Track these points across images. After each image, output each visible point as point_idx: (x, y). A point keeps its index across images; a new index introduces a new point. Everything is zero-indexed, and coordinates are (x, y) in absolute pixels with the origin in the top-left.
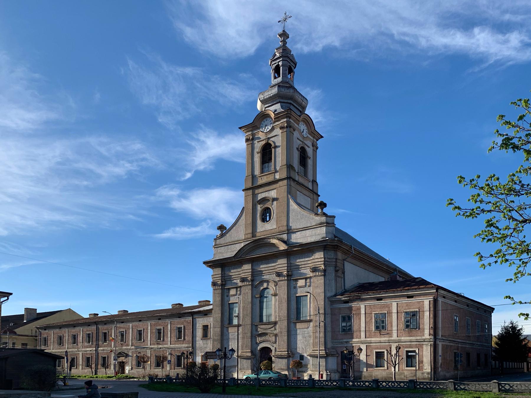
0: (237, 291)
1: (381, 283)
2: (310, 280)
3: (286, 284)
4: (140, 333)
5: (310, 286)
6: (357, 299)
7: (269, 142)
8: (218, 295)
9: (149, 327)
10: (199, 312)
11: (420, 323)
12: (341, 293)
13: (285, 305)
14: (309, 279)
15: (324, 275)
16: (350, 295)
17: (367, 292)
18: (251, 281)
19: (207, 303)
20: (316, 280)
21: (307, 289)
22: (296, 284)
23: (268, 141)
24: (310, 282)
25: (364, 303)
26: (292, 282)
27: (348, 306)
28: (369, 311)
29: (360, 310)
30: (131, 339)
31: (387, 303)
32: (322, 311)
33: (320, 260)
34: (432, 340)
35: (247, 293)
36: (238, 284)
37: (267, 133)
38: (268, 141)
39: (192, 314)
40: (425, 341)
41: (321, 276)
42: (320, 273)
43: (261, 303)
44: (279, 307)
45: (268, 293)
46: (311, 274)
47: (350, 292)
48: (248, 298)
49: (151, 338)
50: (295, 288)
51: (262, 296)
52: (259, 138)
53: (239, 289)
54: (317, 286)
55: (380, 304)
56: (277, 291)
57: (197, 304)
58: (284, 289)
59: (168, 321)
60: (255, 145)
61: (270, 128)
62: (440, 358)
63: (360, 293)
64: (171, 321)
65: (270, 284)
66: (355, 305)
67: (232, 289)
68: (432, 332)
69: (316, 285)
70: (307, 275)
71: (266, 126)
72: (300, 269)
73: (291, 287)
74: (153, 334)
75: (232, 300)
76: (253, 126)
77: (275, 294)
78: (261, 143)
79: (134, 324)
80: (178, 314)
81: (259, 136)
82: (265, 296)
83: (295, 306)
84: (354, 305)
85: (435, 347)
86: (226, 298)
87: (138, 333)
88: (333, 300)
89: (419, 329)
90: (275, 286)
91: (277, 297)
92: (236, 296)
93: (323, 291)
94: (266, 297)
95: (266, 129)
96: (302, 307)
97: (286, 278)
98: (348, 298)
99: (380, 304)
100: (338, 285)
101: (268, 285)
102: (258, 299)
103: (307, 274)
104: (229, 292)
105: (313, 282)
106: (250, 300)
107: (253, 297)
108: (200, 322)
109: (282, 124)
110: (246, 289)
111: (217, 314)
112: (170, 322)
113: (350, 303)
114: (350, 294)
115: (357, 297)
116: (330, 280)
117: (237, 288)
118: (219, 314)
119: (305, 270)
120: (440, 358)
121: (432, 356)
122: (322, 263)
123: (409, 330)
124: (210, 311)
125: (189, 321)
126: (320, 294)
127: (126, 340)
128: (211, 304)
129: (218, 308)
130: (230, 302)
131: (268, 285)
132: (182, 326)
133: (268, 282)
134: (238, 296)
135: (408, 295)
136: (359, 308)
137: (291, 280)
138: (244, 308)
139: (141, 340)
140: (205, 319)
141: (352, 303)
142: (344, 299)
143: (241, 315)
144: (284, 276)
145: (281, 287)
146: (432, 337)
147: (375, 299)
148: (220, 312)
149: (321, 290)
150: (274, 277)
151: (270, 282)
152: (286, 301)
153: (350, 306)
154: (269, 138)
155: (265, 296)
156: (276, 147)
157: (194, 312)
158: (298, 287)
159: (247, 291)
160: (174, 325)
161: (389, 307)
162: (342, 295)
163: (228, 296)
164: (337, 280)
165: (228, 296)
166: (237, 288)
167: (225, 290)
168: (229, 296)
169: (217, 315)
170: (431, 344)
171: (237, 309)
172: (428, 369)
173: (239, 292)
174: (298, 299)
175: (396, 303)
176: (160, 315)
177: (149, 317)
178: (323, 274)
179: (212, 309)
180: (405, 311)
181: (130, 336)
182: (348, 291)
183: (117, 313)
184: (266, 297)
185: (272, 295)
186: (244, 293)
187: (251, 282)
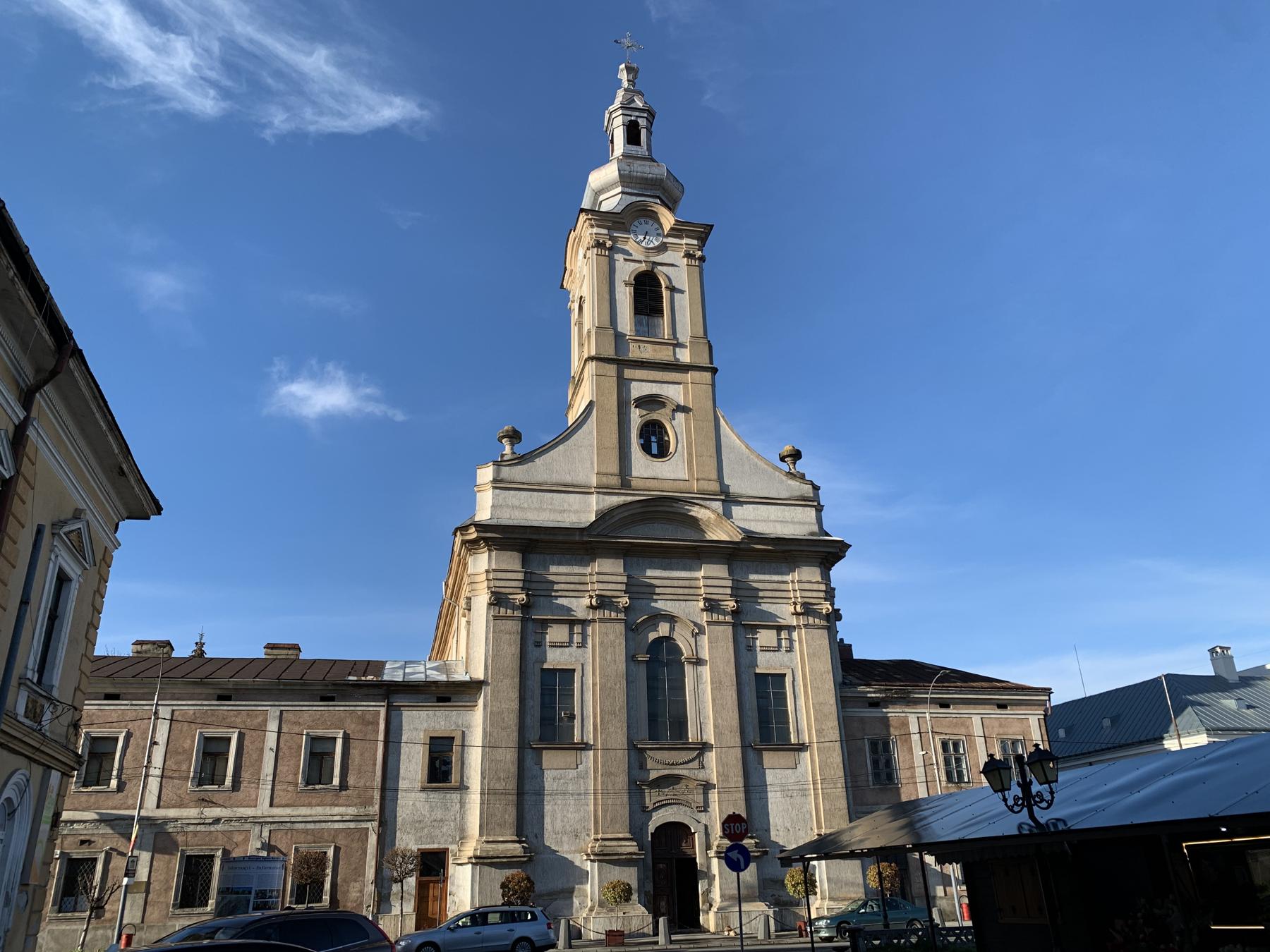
0: (571, 634)
2: (790, 635)
7: (655, 270)
14: (787, 631)
17: (922, 684)
18: (623, 610)
21: (782, 657)
22: (752, 638)
24: (791, 640)
27: (880, 715)
31: (962, 716)
33: (815, 587)
35: (612, 644)
36: (573, 613)
37: (650, 251)
38: (653, 269)
41: (822, 627)
42: (817, 621)
48: (615, 661)
53: (577, 629)
58: (725, 648)
61: (657, 244)
64: (281, 712)
66: (897, 715)
67: (555, 626)
69: (811, 650)
71: (646, 234)
72: (759, 601)
74: (180, 757)
76: (616, 220)
78: (632, 264)
84: (893, 715)
86: (533, 653)
88: (849, 695)
90: (695, 635)
91: (706, 671)
92: (567, 650)
93: (831, 668)
94: (667, 665)
95: (646, 240)
97: (729, 618)
98: (884, 695)
101: (672, 629)
107: (631, 658)
109: (687, 246)
112: (278, 713)
113: (886, 708)
115: (903, 693)
117: (572, 623)
119: (774, 606)
126: (824, 677)
130: (545, 666)
131: (672, 629)
133: (672, 619)
142: (873, 695)
144: (725, 613)
147: (936, 703)
148: (515, 695)
150: (694, 610)
151: (676, 622)
158: (758, 649)
159: (611, 637)
161: (965, 724)
165: (540, 646)
167: (530, 625)
168: (543, 647)
169: (503, 706)
183: (260, 653)
187: (623, 614)
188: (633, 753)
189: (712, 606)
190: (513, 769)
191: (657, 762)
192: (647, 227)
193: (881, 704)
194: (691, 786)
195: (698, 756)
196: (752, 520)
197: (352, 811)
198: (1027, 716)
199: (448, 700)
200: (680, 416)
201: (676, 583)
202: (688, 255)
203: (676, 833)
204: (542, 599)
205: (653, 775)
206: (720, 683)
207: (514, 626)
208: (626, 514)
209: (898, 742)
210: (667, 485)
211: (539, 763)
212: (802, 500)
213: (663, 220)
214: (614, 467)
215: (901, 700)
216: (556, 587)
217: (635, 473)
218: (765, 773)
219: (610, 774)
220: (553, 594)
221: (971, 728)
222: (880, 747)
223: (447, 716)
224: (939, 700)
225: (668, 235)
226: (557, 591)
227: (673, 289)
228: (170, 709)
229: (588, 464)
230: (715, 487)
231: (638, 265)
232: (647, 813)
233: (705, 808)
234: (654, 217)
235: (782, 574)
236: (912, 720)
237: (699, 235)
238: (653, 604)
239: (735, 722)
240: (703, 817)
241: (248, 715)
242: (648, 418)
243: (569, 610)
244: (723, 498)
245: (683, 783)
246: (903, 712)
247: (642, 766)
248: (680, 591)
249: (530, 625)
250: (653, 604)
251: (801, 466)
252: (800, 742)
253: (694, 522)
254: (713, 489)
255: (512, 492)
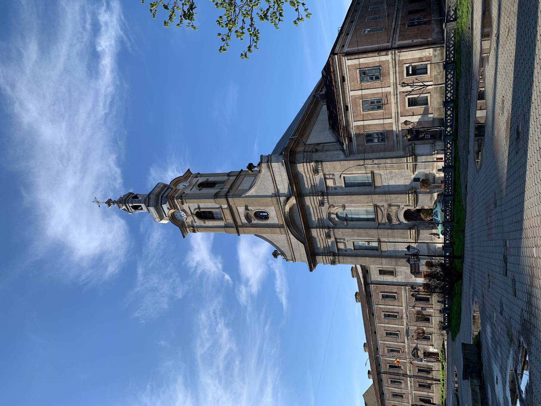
0: (341, 242)
1: (328, 109)
3: (332, 197)
4: (389, 334)
5: (333, 175)
6: (346, 130)
7: (195, 213)
8: (345, 260)
9: (382, 326)
10: (365, 277)
11: (373, 66)
12: (341, 145)
13: (355, 197)
15: (322, 162)
16: (343, 137)
19: (354, 269)
20: (327, 170)
21: (337, 177)
23: (194, 214)
24: (329, 175)
25: (351, 123)
26: (329, 192)
27: (355, 138)
28: (360, 117)
29: (359, 126)
30: (396, 343)
32: (361, 162)
34: (393, 52)
35: (342, 233)
38: (194, 214)
39: (367, 284)
40: (395, 59)
43: (352, 220)
44: (358, 203)
45: (342, 214)
46: (321, 174)
47: (339, 137)
48: (348, 232)
49: (395, 324)
50: (335, 188)
51: (346, 219)
52: (192, 222)
54: (334, 168)
55: (352, 108)
56: (339, 205)
57: (355, 279)
59: (375, 307)
60: (198, 225)
61: (183, 213)
62: (415, 41)
63: (341, 127)
65: (331, 212)
66: (354, 131)
68: (384, 53)
70: (322, 177)
73: (336, 192)
75: (350, 246)
77: (343, 207)
78: (196, 221)
79: (379, 339)
80: (367, 297)
81: (190, 222)
82: (345, 216)
83: (356, 188)
85: (401, 48)
87: (390, 336)
89: (381, 66)
90: (334, 207)
91: (346, 205)
92: (346, 243)
94: (347, 215)
96: (357, 182)
97: (325, 197)
99: (352, 108)
100: (331, 149)
101: (333, 214)
102: (349, 222)
103: (321, 178)
104: (342, 249)
105: (329, 172)
106: (350, 230)
107: (346, 227)
108: (375, 276)
110: (338, 233)
111: (366, 261)
114: (342, 136)
116: (327, 157)
117: (337, 242)
118: (366, 259)
120: (415, 41)
121: (413, 49)
122: (308, 164)
123: (381, 76)
124: (363, 268)
125: (375, 288)
127: (398, 347)
128: (356, 266)
129: (360, 260)
130: (353, 249)
131: (333, 214)
132: (381, 294)
133: (330, 214)
134: (346, 242)
135: (342, 81)
136: (357, 127)
137: (327, 193)
138: (358, 236)
139: (398, 333)
140: (372, 272)
141: (351, 134)
142: (347, 142)
143: (367, 239)
145: (335, 201)
146: (390, 52)
148: (364, 258)
149: (337, 164)
150: (325, 209)
152: (350, 196)
153: (355, 136)
154: (192, 214)
155: (345, 216)
156: (199, 208)
157: (364, 282)
159: (340, 233)
160: (380, 302)
162: (343, 144)
163: (346, 251)
164: (327, 149)
166: (337, 242)
170: (398, 52)
171: (360, 243)
172: (430, 51)
173: (342, 241)
174: (346, 185)
175: (350, 92)
176: (369, 314)
177: (370, 324)
178: (320, 163)
179: (361, 266)
180: (359, 83)
181: (392, 343)
182: (338, 139)
184: (347, 215)
185: (344, 209)
186: (343, 236)
188: (380, 226)
189: (322, 204)
190: (388, 259)
191: (382, 220)
192: (179, 216)
193: (350, 137)
194: (390, 210)
195: (379, 207)
196: (284, 187)
197: (403, 291)
198: (347, 66)
199: (367, 271)
200: (249, 208)
201: (315, 212)
202: (182, 203)
203: (408, 215)
204: (330, 249)
205: (387, 221)
206: (351, 201)
207: (341, 258)
208: (295, 231)
209: (366, 131)
210: (279, 214)
211: (386, 251)
212: (270, 169)
213: (173, 211)
214: (278, 229)
215: (347, 128)
216: (325, 246)
217: (277, 222)
218: (384, 186)
219: (388, 235)
220: (328, 246)
221: (356, 97)
222: (369, 138)
223: (373, 271)
224: (345, 111)
225: (178, 209)
226: (326, 245)
227: (199, 208)
228: (377, 324)
229: (279, 236)
230: (274, 199)
231: (195, 219)
232: (401, 223)
233: (399, 206)
234: (173, 214)
235: (302, 176)
236: (355, 124)
237: (172, 200)
238: (325, 218)
239: (365, 196)
240: (402, 206)
241: (377, 310)
242: (254, 218)
243: (332, 242)
244: (278, 197)
245: (389, 212)
246: (353, 128)
247: (384, 224)
248: (318, 211)
249: (340, 253)
250: (325, 218)
251: (255, 164)
252: (370, 172)
253: (291, 209)
254: (275, 200)
255: (295, 257)
